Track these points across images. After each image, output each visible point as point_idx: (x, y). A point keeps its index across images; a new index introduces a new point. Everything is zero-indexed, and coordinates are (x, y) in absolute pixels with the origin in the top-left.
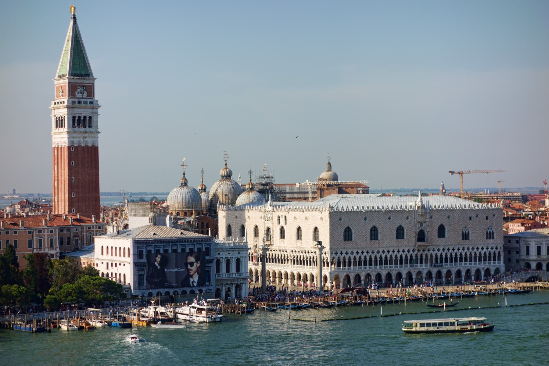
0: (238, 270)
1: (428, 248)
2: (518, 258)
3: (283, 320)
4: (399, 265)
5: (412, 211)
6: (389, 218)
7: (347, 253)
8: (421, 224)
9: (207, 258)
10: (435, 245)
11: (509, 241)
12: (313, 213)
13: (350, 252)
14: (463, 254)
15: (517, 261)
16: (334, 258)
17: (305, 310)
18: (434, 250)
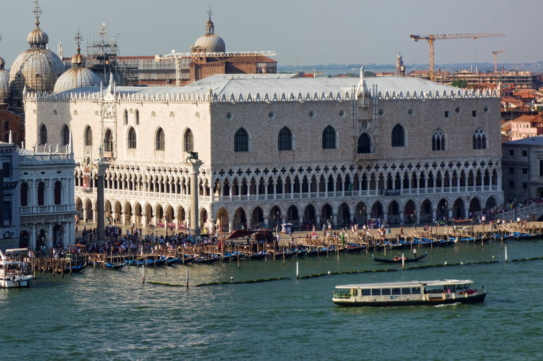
0: (57, 200)
1: (375, 163)
2: (526, 180)
3: (133, 284)
4: (326, 192)
5: (349, 101)
6: (311, 114)
7: (240, 172)
8: (364, 123)
9: (6, 180)
10: (387, 159)
11: (512, 153)
12: (183, 105)
13: (244, 170)
14: (435, 174)
15: (525, 185)
16: (218, 180)
17: (169, 268)
18: (385, 167)
